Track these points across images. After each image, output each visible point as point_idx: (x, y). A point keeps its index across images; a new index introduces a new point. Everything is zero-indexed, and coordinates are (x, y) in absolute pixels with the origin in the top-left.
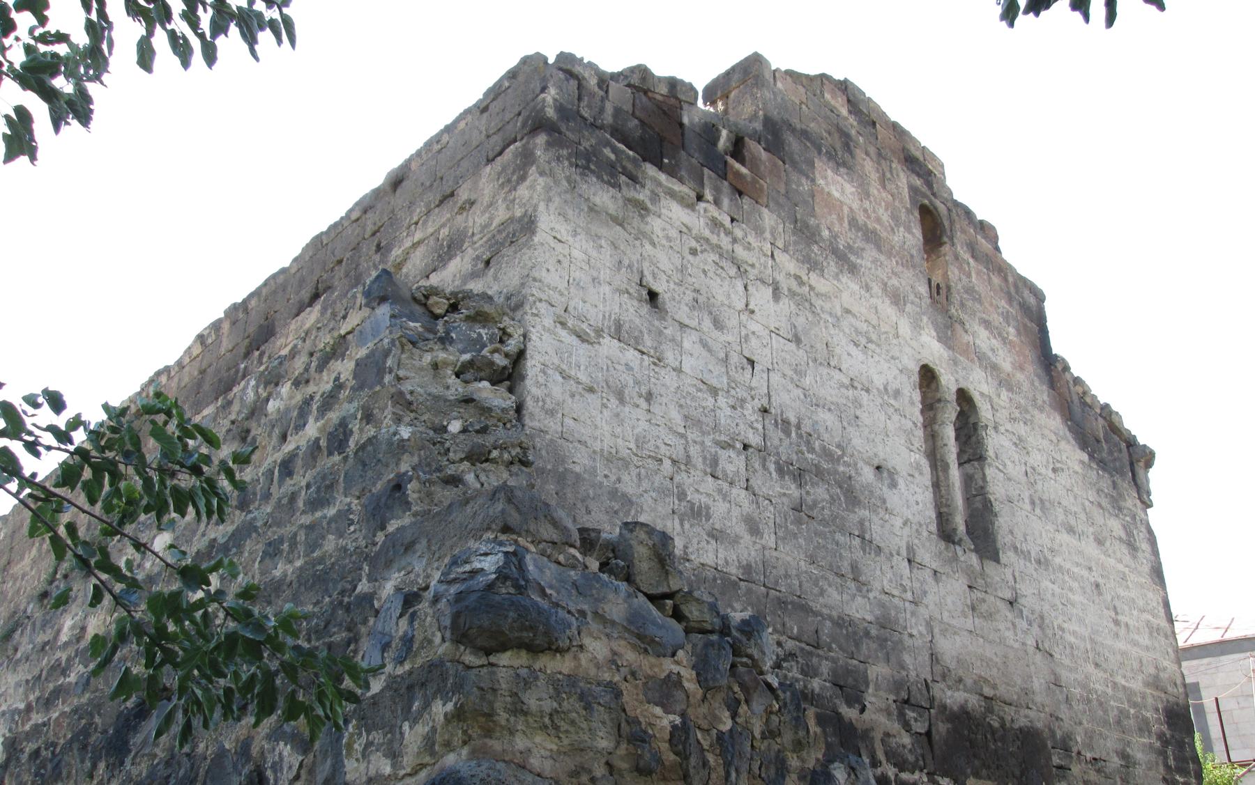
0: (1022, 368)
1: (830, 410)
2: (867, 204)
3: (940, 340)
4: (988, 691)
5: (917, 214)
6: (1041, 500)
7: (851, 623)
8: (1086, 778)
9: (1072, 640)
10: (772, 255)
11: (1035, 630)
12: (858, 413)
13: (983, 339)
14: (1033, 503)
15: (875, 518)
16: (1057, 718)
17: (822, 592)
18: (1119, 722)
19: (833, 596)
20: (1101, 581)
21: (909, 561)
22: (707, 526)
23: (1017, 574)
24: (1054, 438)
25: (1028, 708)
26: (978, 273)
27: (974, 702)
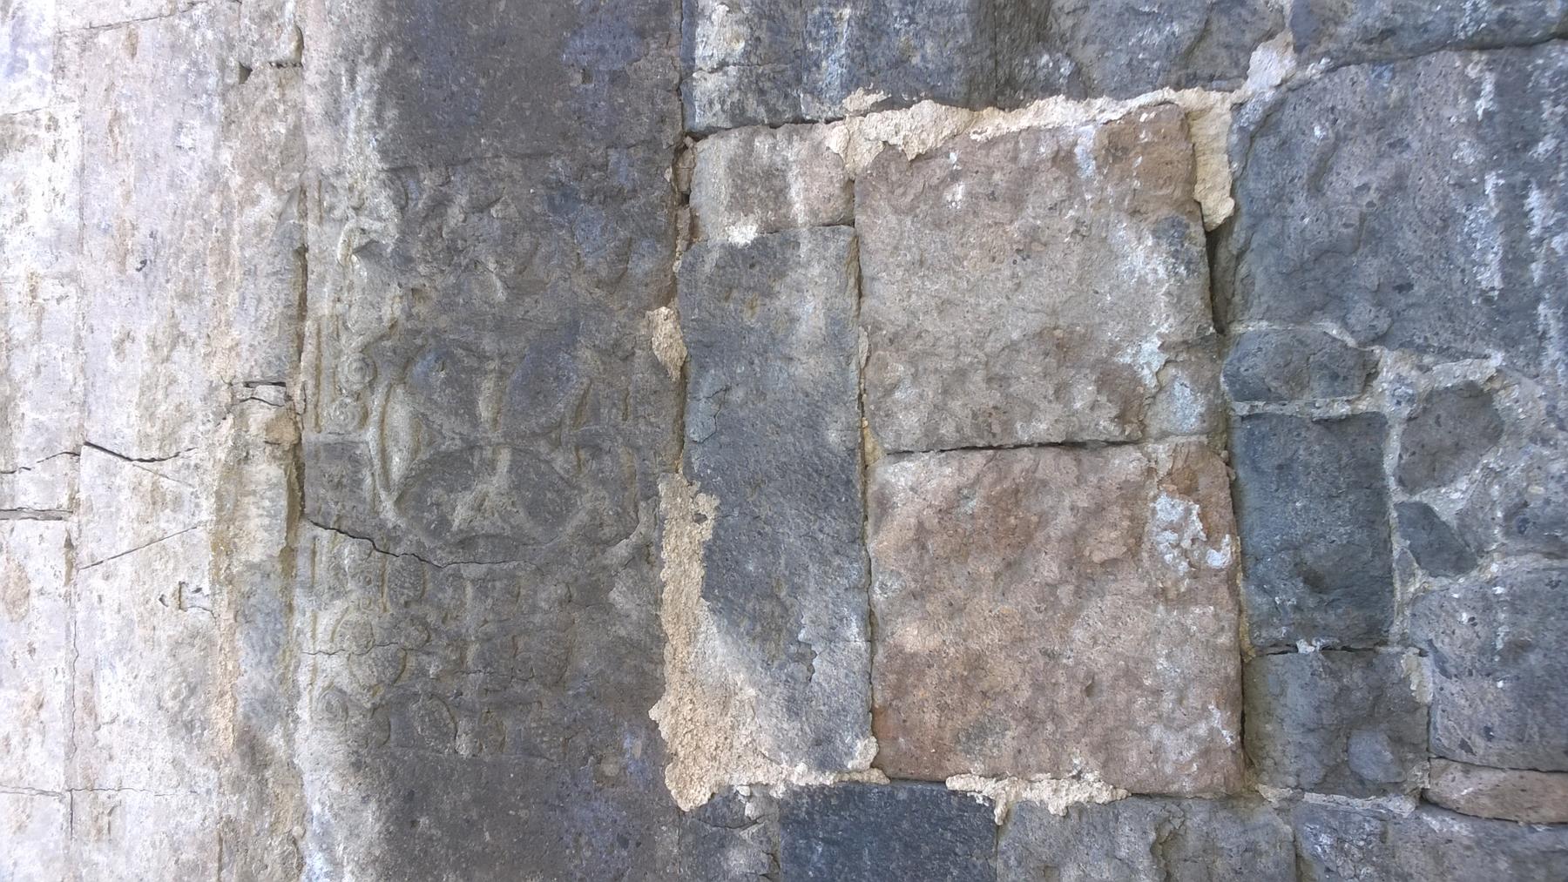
4: (260, 536)
25: (292, 66)
27: (327, 644)
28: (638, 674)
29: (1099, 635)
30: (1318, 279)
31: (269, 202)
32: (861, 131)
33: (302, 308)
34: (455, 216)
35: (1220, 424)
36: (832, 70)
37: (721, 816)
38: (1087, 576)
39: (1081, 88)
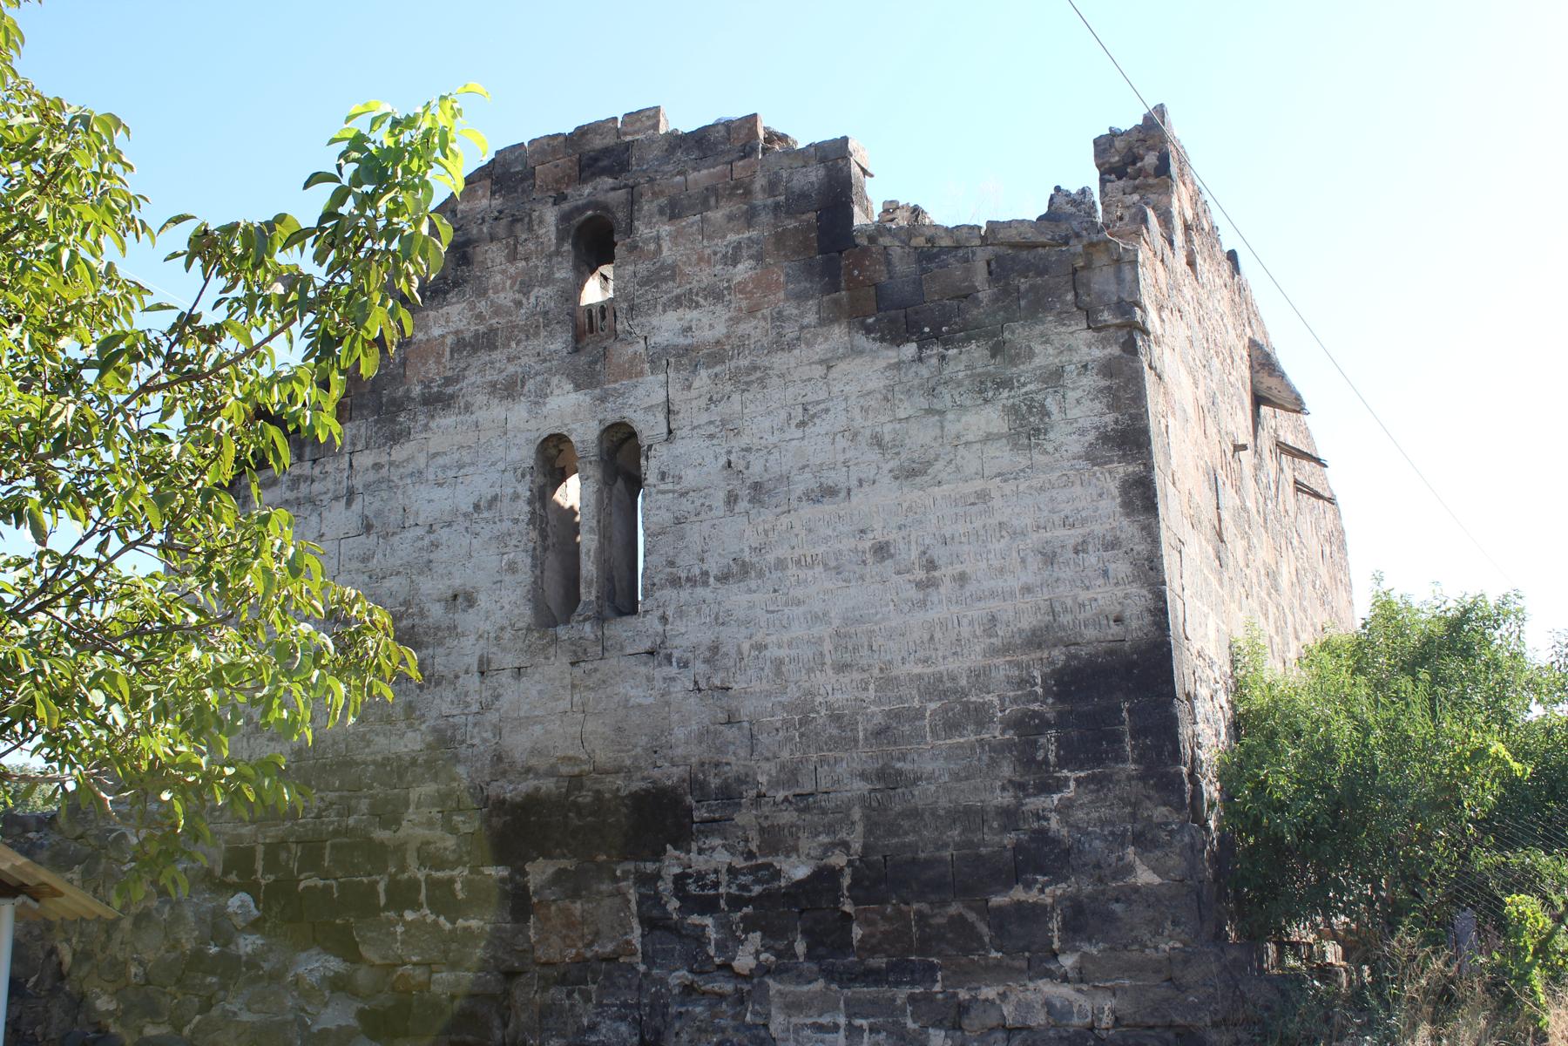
0: (752, 312)
1: (398, 573)
2: (482, 306)
3: (578, 387)
4: (565, 770)
5: (567, 247)
6: (757, 486)
7: (399, 758)
8: (765, 824)
9: (782, 653)
10: (351, 465)
11: (700, 667)
12: (432, 556)
13: (666, 326)
14: (732, 499)
15: (440, 651)
16: (717, 765)
17: (369, 743)
18: (880, 733)
19: (381, 741)
20: (891, 537)
21: (482, 673)
22: (268, 735)
23: (670, 613)
24: (819, 370)
26: (675, 238)
27: (548, 785)
28: (548, 856)
29: (555, 940)
30: (608, 976)
31: (628, 762)
32: (633, 896)
33: (607, 773)
34: (624, 810)
35: (588, 960)
36: (643, 890)
37: (525, 874)
38: (564, 938)
39: (643, 936)
